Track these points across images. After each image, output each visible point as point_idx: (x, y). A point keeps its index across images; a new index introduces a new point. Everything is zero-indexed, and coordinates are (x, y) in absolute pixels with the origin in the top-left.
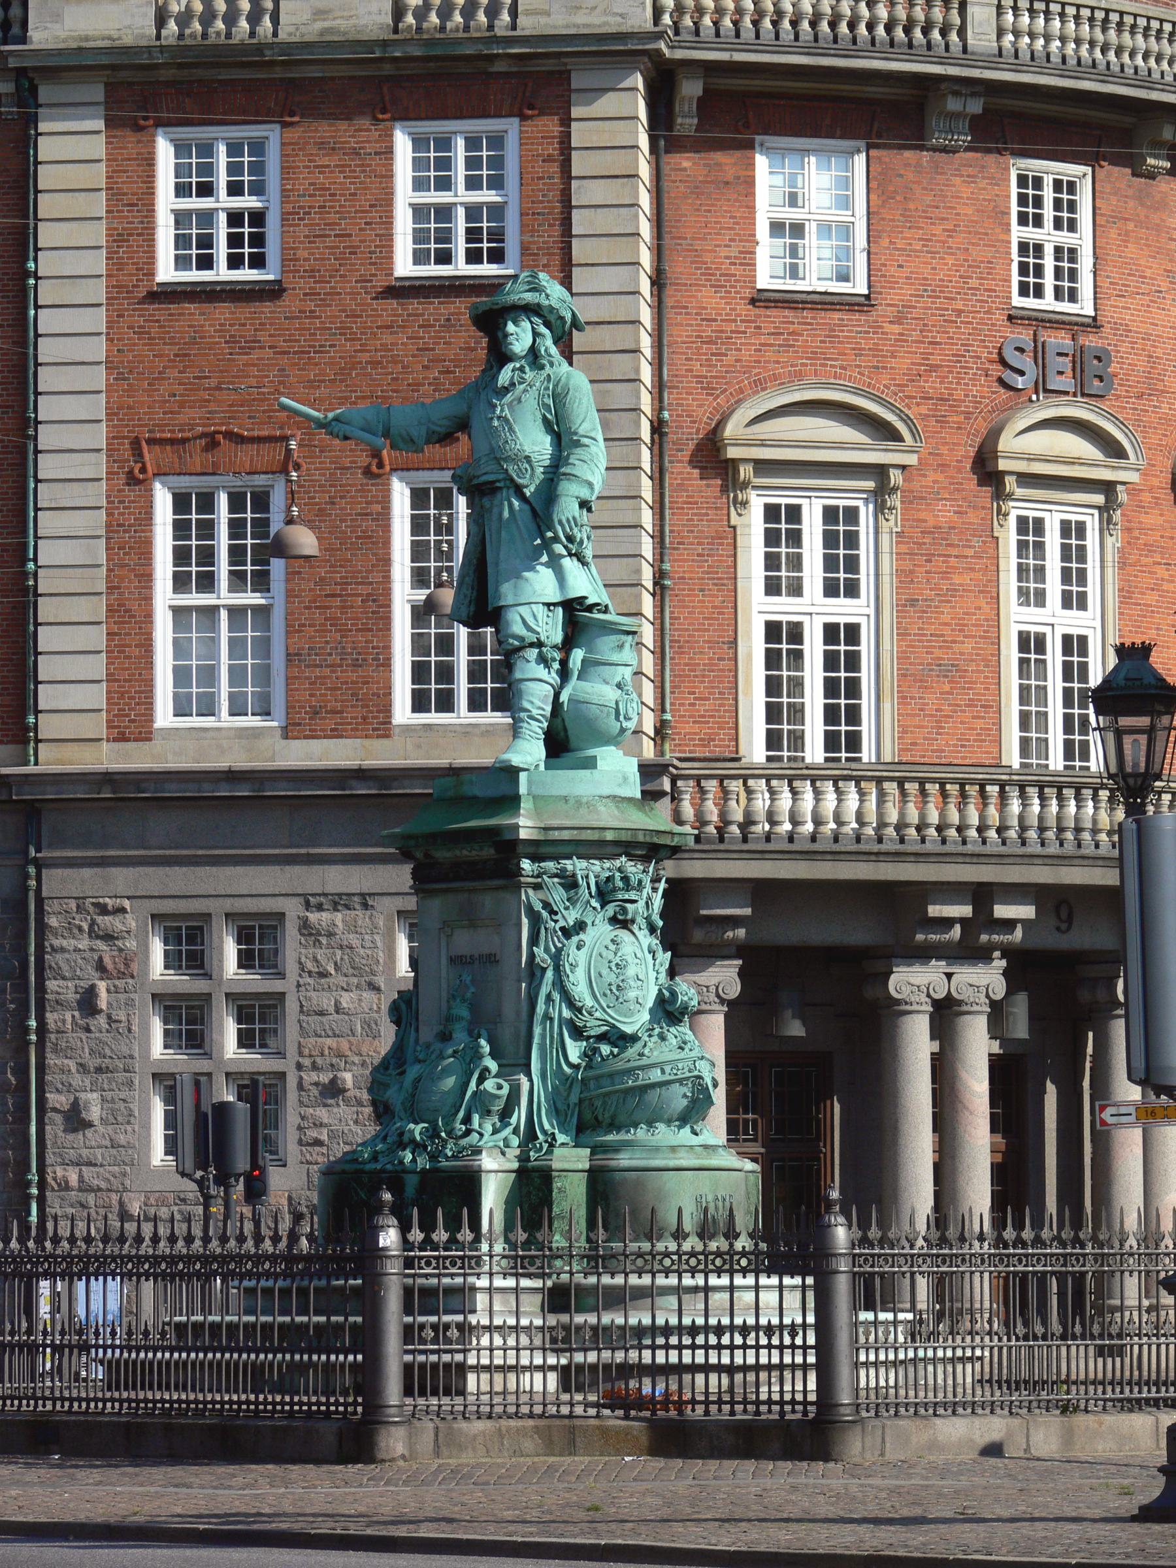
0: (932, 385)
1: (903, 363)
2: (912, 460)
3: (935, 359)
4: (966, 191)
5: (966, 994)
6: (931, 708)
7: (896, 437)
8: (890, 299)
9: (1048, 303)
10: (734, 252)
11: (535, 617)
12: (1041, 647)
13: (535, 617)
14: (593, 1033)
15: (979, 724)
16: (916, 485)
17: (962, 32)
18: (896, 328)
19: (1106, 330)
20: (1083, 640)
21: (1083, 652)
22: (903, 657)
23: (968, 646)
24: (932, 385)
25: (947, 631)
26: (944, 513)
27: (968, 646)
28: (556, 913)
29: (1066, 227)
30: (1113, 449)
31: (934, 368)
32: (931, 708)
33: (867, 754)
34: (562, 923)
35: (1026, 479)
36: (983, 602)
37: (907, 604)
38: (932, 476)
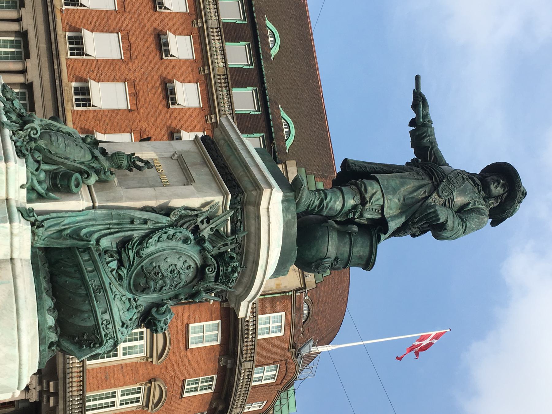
0: (170, 365)
1: (174, 358)
2: (154, 363)
3: (175, 365)
4: (210, 367)
5: (30, 394)
6: (98, 375)
7: (159, 359)
8: (188, 353)
9: (186, 387)
10: (198, 318)
11: (377, 200)
12: (112, 397)
13: (377, 200)
14: (124, 255)
15: (95, 386)
16: (148, 365)
17: (246, 361)
18: (182, 356)
19: (180, 400)
20: (114, 406)
21: (111, 406)
22: (110, 367)
23: (113, 381)
24: (170, 365)
25: (116, 376)
26: (142, 371)
27: (113, 381)
28: (208, 222)
29: (201, 387)
30: (156, 405)
31: (173, 365)
32: (98, 375)
33: (88, 363)
34: (202, 227)
35: (150, 389)
36: (122, 383)
37: (122, 366)
38: (150, 368)
